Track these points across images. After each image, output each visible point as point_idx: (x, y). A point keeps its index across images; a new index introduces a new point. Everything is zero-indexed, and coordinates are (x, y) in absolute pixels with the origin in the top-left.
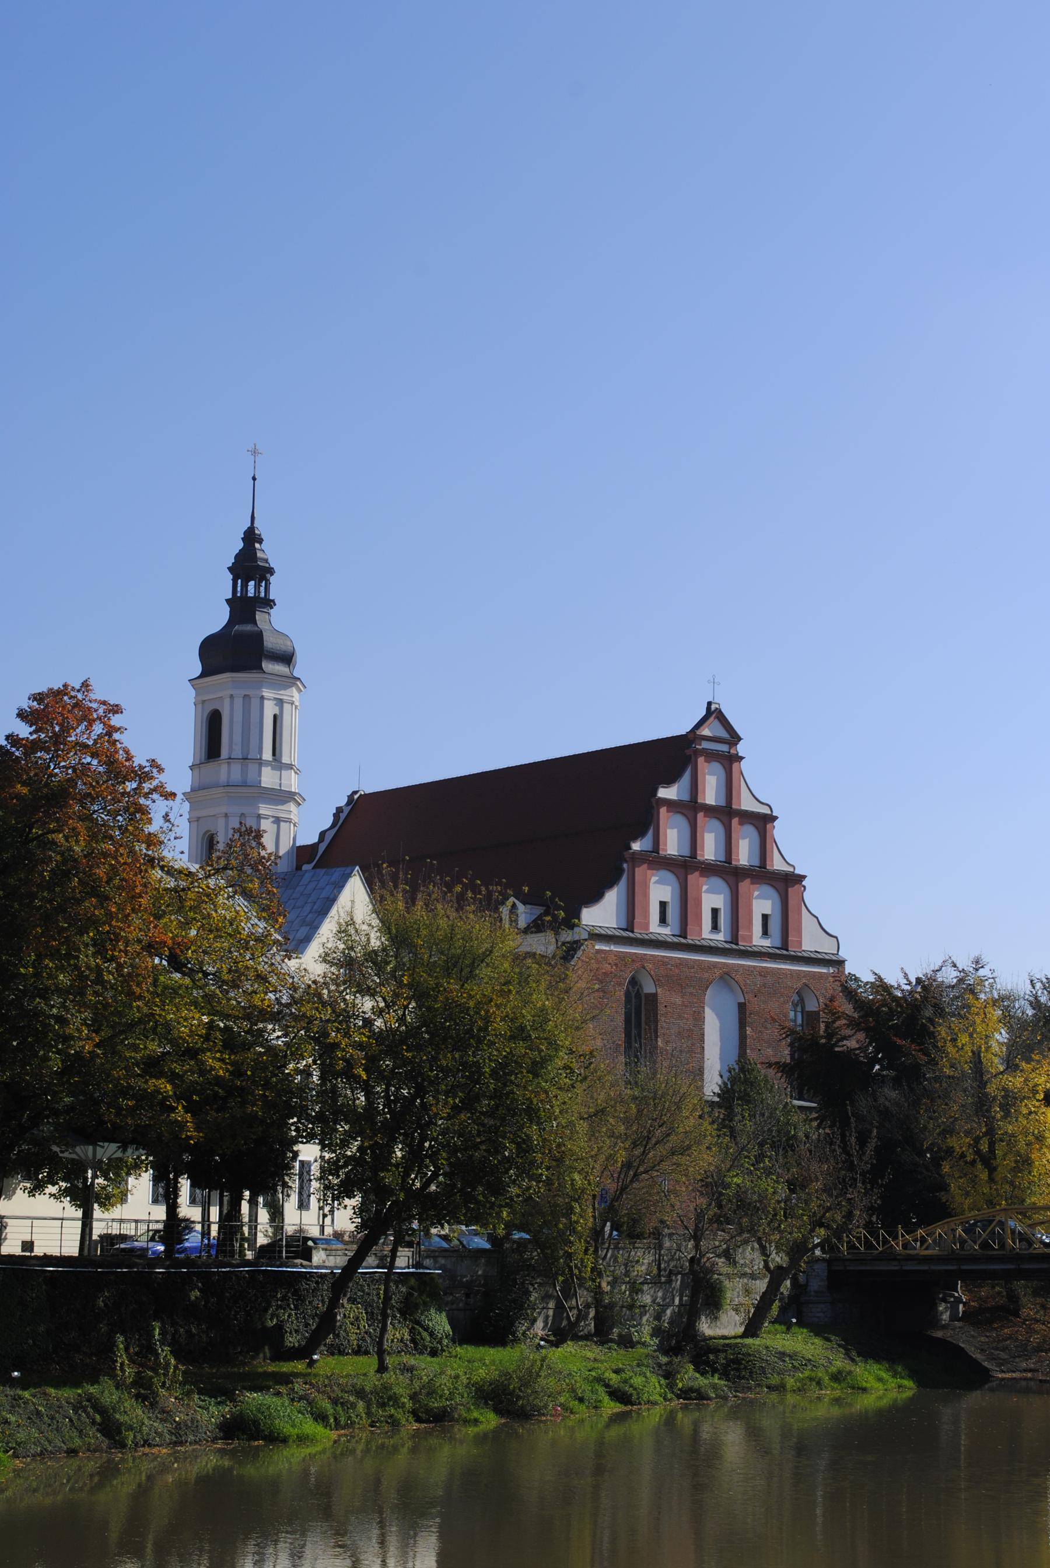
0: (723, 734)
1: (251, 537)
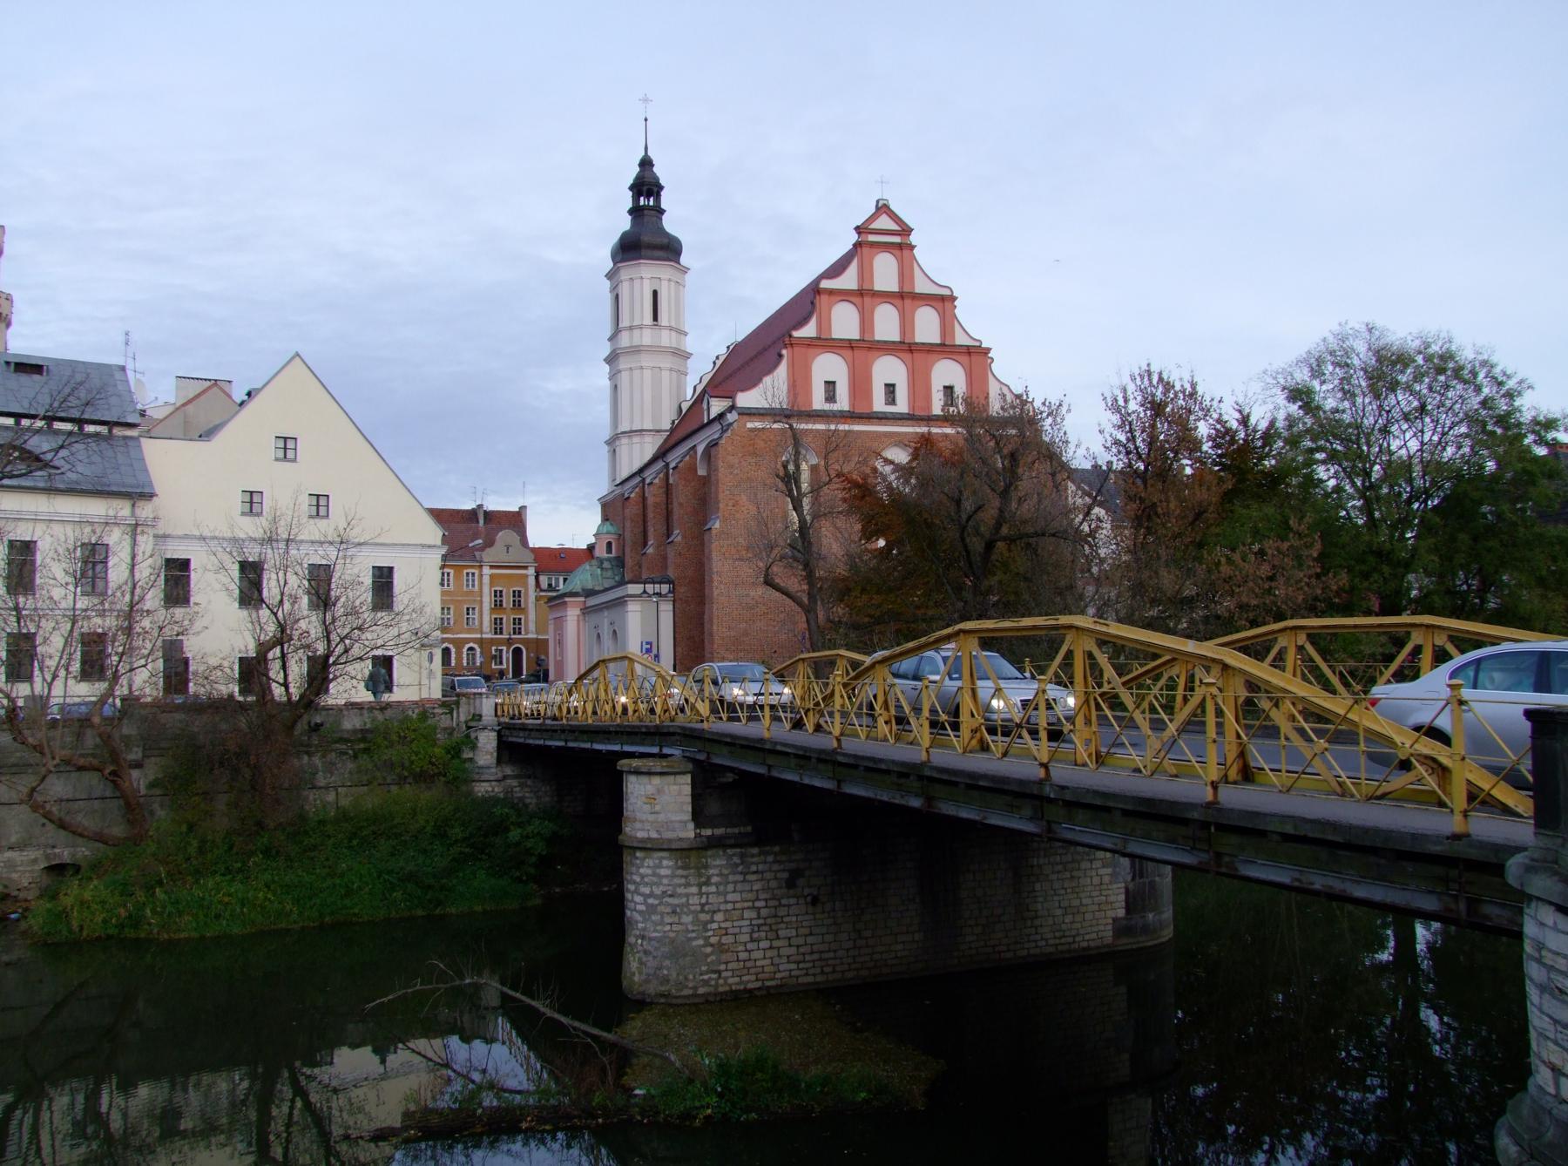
0: (895, 227)
1: (646, 163)
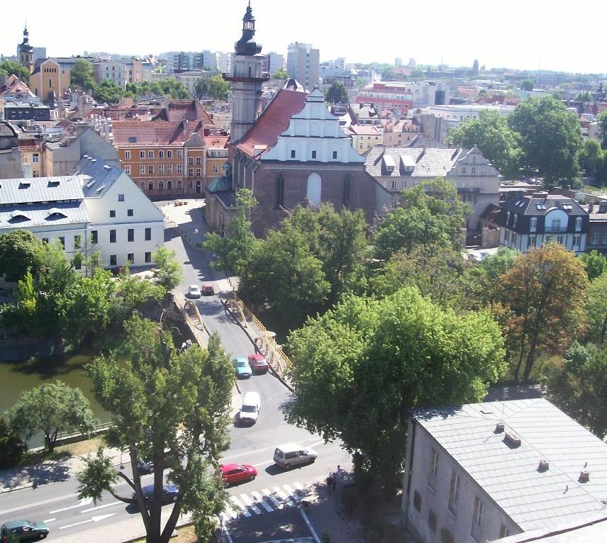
1: (249, 10)
